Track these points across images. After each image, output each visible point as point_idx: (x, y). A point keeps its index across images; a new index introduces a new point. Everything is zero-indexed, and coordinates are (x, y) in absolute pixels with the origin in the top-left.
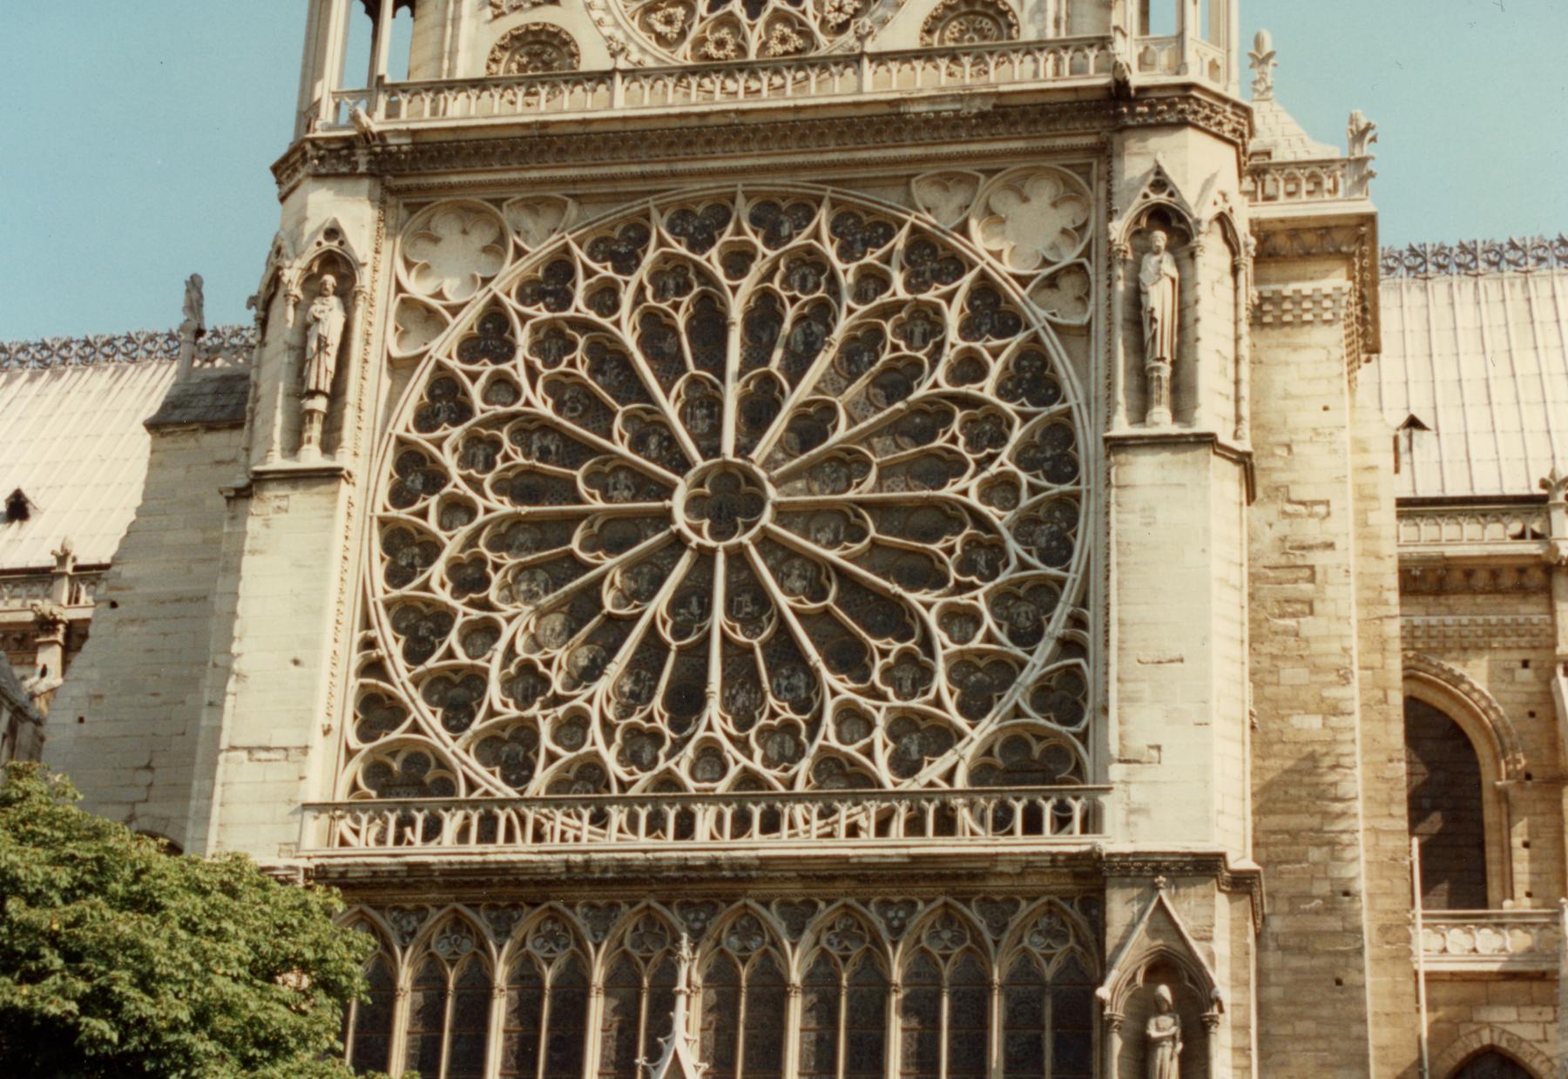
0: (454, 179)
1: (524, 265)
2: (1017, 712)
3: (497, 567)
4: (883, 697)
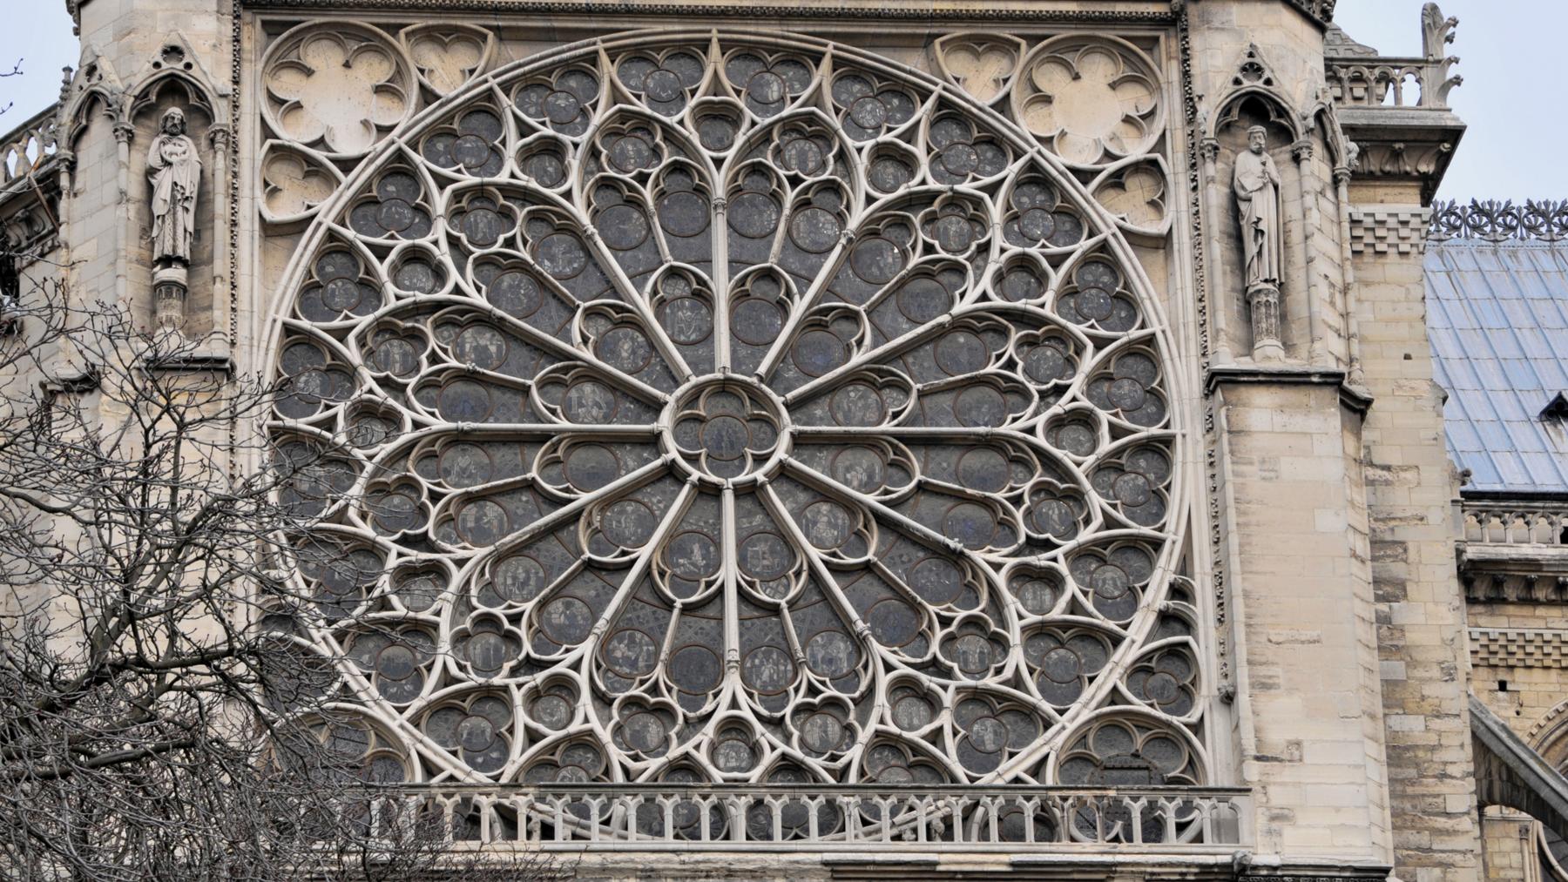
1: (432, 113)
2: (1115, 696)
4: (948, 673)
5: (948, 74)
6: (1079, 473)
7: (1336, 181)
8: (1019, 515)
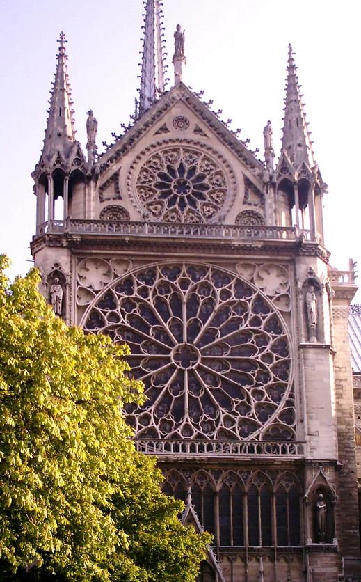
0: (94, 251)
1: (117, 280)
2: (276, 420)
4: (237, 415)
5: (239, 272)
6: (268, 368)
8: (254, 378)
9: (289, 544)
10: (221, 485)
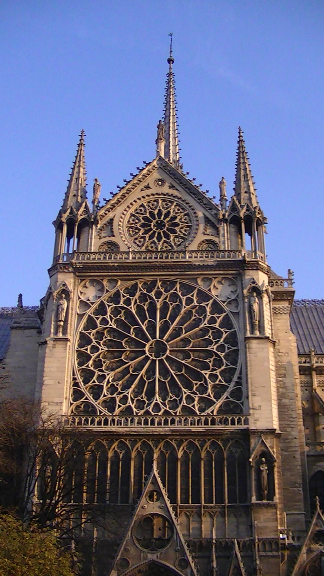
2: (227, 398)
3: (104, 362)
4: (196, 394)
6: (222, 356)
7: (270, 301)
9: (238, 501)
10: (182, 452)
